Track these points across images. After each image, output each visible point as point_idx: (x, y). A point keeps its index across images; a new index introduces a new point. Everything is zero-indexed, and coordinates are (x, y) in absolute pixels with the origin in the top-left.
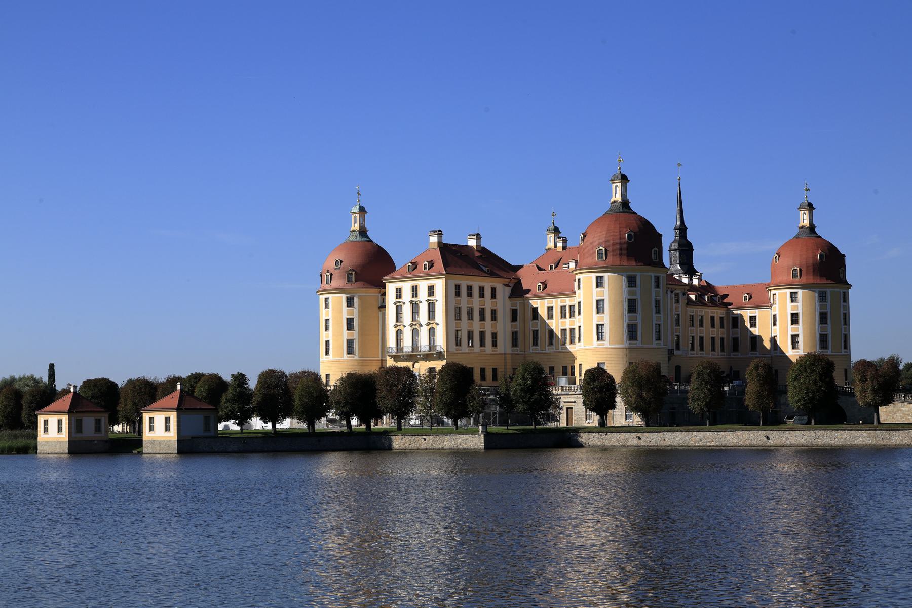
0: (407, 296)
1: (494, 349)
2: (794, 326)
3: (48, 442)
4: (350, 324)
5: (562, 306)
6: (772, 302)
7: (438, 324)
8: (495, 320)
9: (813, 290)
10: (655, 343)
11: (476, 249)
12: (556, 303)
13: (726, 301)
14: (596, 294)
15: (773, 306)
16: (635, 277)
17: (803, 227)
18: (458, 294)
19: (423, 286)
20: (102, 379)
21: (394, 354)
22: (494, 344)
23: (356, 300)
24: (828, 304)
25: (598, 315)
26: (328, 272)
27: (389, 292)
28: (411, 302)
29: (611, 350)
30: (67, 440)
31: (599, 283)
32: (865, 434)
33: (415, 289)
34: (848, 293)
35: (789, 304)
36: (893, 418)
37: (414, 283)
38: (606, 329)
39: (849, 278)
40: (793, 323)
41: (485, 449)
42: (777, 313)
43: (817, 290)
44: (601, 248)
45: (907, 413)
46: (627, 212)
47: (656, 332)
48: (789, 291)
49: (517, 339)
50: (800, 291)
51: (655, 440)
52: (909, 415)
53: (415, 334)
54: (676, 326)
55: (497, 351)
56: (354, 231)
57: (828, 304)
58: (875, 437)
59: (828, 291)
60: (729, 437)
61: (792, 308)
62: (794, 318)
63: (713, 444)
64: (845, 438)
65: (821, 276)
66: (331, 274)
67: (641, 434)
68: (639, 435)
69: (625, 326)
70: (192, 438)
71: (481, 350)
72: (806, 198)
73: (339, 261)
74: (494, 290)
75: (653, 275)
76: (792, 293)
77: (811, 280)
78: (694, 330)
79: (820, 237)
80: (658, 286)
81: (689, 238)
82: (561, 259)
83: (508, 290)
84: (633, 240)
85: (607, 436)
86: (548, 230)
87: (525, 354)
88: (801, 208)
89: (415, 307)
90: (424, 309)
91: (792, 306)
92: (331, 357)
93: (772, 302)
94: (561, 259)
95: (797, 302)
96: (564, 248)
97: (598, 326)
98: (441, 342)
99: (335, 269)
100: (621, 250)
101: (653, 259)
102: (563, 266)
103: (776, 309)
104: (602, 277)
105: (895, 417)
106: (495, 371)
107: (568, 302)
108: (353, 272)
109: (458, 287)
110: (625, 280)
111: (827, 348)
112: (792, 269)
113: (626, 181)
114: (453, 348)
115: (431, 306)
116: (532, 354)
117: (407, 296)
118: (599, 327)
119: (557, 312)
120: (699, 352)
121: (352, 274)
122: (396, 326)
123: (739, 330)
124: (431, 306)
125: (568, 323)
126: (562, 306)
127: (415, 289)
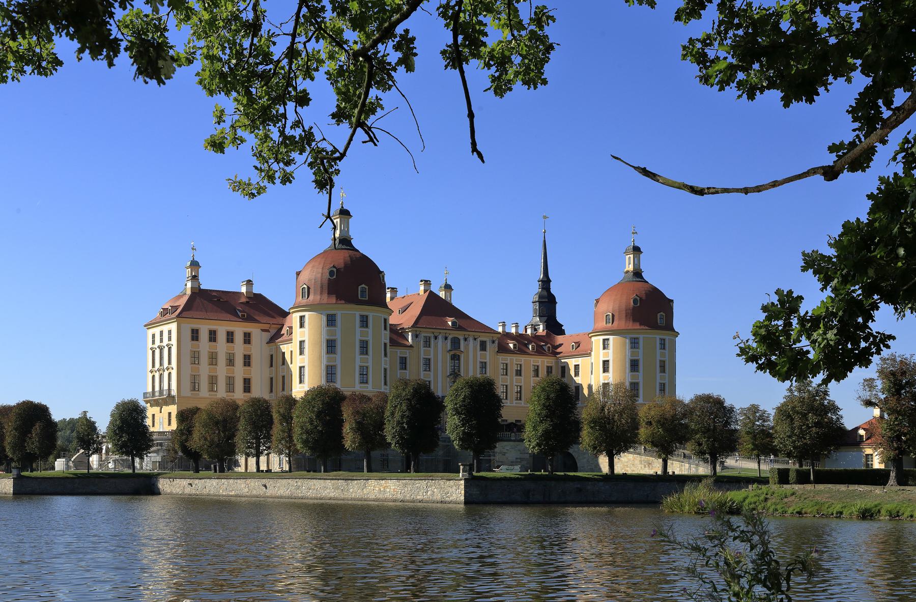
8: (249, 365)
13: (559, 350)
22: (247, 388)
24: (641, 351)
32: (330, 484)
33: (161, 333)
39: (676, 326)
41: (467, 502)
42: (593, 361)
44: (609, 313)
47: (661, 390)
50: (611, 338)
61: (605, 355)
63: (233, 493)
65: (634, 320)
69: (324, 367)
71: (227, 396)
75: (358, 314)
79: (648, 282)
81: (552, 291)
84: (335, 277)
88: (626, 253)
100: (322, 287)
101: (359, 296)
104: (608, 339)
110: (324, 318)
111: (367, 383)
113: (349, 217)
114: (187, 392)
122: (151, 372)
123: (407, 372)
127: (161, 333)
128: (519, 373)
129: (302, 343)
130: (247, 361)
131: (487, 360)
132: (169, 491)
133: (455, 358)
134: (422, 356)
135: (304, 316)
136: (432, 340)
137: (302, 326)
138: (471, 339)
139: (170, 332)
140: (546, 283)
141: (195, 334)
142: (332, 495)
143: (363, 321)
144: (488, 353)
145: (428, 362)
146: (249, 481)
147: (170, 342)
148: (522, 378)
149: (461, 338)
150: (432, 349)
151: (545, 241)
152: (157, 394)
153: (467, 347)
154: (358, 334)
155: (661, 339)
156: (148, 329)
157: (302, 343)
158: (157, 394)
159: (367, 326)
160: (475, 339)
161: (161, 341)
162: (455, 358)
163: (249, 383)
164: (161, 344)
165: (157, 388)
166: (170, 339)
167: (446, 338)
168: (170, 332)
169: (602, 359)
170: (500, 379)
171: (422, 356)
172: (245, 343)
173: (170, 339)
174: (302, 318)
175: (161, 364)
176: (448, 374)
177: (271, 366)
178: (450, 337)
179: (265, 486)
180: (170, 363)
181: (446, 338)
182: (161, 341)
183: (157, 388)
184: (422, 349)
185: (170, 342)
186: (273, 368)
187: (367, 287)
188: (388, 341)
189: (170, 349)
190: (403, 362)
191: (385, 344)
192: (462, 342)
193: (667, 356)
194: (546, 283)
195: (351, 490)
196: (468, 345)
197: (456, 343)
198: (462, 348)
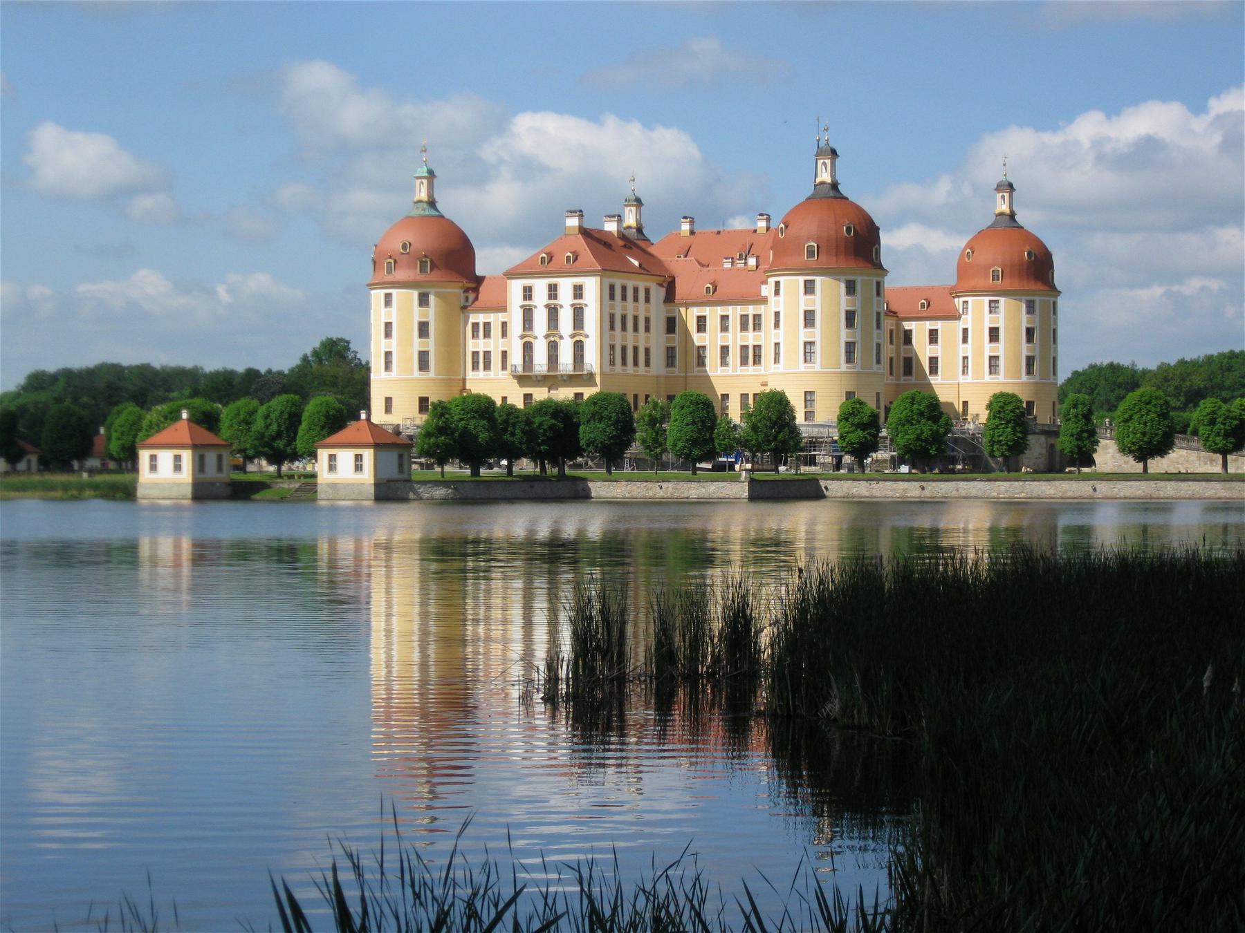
0: (540, 297)
1: (647, 369)
2: (993, 345)
3: (156, 484)
4: (423, 329)
5: (742, 316)
6: (961, 312)
7: (587, 336)
9: (838, 277)
10: (875, 366)
11: (616, 235)
12: (734, 312)
14: (804, 302)
15: (963, 317)
16: (1033, 302)
17: (1001, 214)
18: (612, 297)
19: (566, 286)
21: (521, 373)
22: (647, 363)
23: (432, 298)
25: (807, 330)
26: (390, 257)
27: (536, 296)
28: (547, 306)
29: (829, 375)
30: (373, 482)
31: (809, 288)
33: (553, 291)
34: (884, 282)
35: (987, 316)
36: (1157, 466)
37: (527, 282)
38: (818, 348)
40: (991, 341)
43: (1024, 298)
45: (1175, 460)
46: (1014, 227)
48: (986, 299)
49: (675, 357)
50: (1002, 300)
51: (944, 490)
52: (1178, 463)
53: (553, 348)
56: (420, 201)
58: (1231, 489)
59: (1037, 299)
60: (1044, 488)
61: (991, 320)
62: (994, 334)
63: (1023, 495)
64: (1194, 490)
66: (395, 262)
67: (926, 483)
68: (923, 484)
70: (389, 481)
72: (828, 140)
73: (408, 244)
74: (647, 291)
77: (1016, 284)
82: (690, 247)
83: (663, 292)
85: (878, 485)
86: (626, 201)
87: (686, 377)
89: (553, 312)
90: (566, 317)
91: (990, 318)
92: (394, 373)
93: (961, 312)
94: (690, 247)
95: (998, 314)
96: (692, 232)
97: (806, 343)
98: (592, 358)
99: (402, 253)
102: (725, 260)
103: (967, 321)
105: (1160, 465)
106: (647, 396)
107: (751, 310)
108: (428, 260)
109: (612, 288)
110: (843, 286)
112: (992, 270)
114: (607, 369)
115: (578, 313)
116: (696, 376)
117: (540, 297)
118: (809, 344)
119: (735, 323)
120: (902, 378)
121: (426, 262)
122: (522, 337)
124: (578, 313)
125: (751, 338)
126: (742, 316)
127: (553, 291)
139: (578, 291)
156: (508, 278)
170: (902, 350)
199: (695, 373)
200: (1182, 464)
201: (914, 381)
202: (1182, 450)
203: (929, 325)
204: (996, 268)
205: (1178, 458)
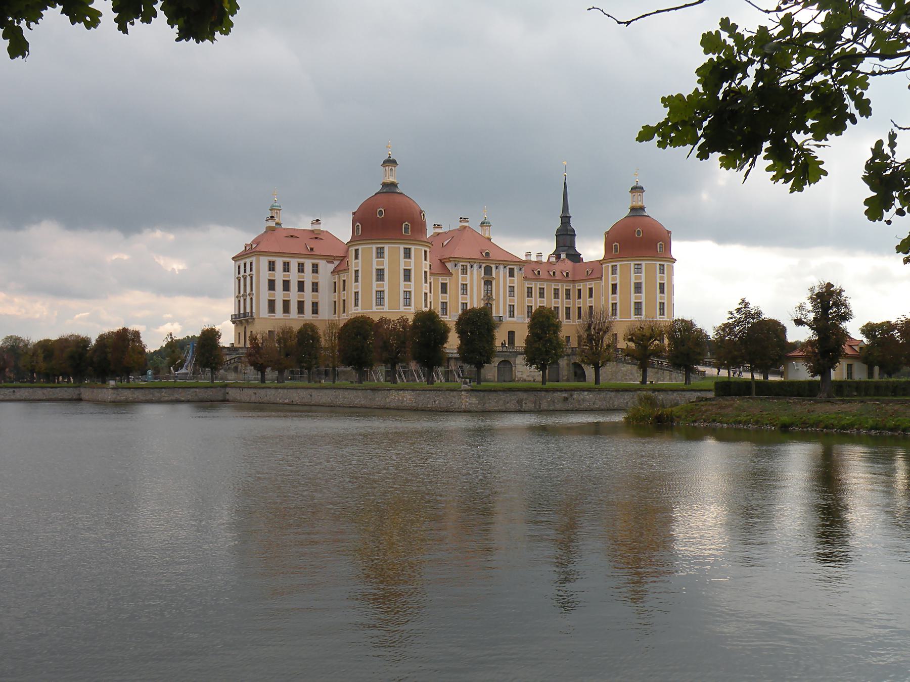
19: (248, 261)
20: (63, 342)
22: (315, 310)
33: (245, 264)
45: (625, 373)
54: (442, 293)
55: (289, 316)
57: (643, 275)
71: (299, 317)
76: (612, 266)
78: (447, 296)
79: (650, 217)
80: (426, 259)
91: (612, 277)
97: (355, 293)
122: (237, 297)
127: (245, 264)
128: (542, 295)
129: (356, 272)
130: (315, 287)
131: (515, 285)
132: (239, 399)
133: (488, 283)
134: (460, 282)
135: (358, 249)
136: (469, 267)
137: (357, 257)
138: (501, 267)
139: (251, 264)
140: (566, 219)
141: (272, 266)
142: (363, 402)
143: (407, 253)
144: (515, 279)
145: (464, 287)
146: (299, 391)
147: (252, 273)
148: (545, 300)
149: (493, 267)
150: (468, 276)
151: (565, 183)
152: (242, 316)
153: (498, 274)
154: (403, 264)
155: (660, 265)
157: (356, 272)
158: (242, 316)
159: (410, 258)
160: (505, 267)
161: (245, 271)
162: (488, 283)
163: (317, 306)
164: (245, 274)
165: (242, 311)
166: (251, 270)
167: (480, 267)
168: (251, 264)
169: (611, 282)
171: (460, 282)
172: (313, 272)
173: (251, 270)
174: (357, 251)
175: (245, 291)
176: (482, 297)
177: (335, 292)
178: (484, 265)
179: (311, 396)
180: (252, 290)
181: (480, 267)
182: (245, 271)
183: (242, 311)
184: (460, 276)
185: (252, 273)
186: (337, 294)
187: (410, 225)
188: (428, 270)
189: (251, 278)
190: (444, 288)
191: (426, 272)
192: (494, 269)
193: (666, 279)
194: (566, 219)
195: (377, 399)
196: (499, 272)
197: (488, 271)
198: (494, 275)
199: (342, 318)
200: (629, 376)
201: (572, 323)
202: (628, 365)
203: (589, 285)
204: (616, 244)
205: (626, 372)
